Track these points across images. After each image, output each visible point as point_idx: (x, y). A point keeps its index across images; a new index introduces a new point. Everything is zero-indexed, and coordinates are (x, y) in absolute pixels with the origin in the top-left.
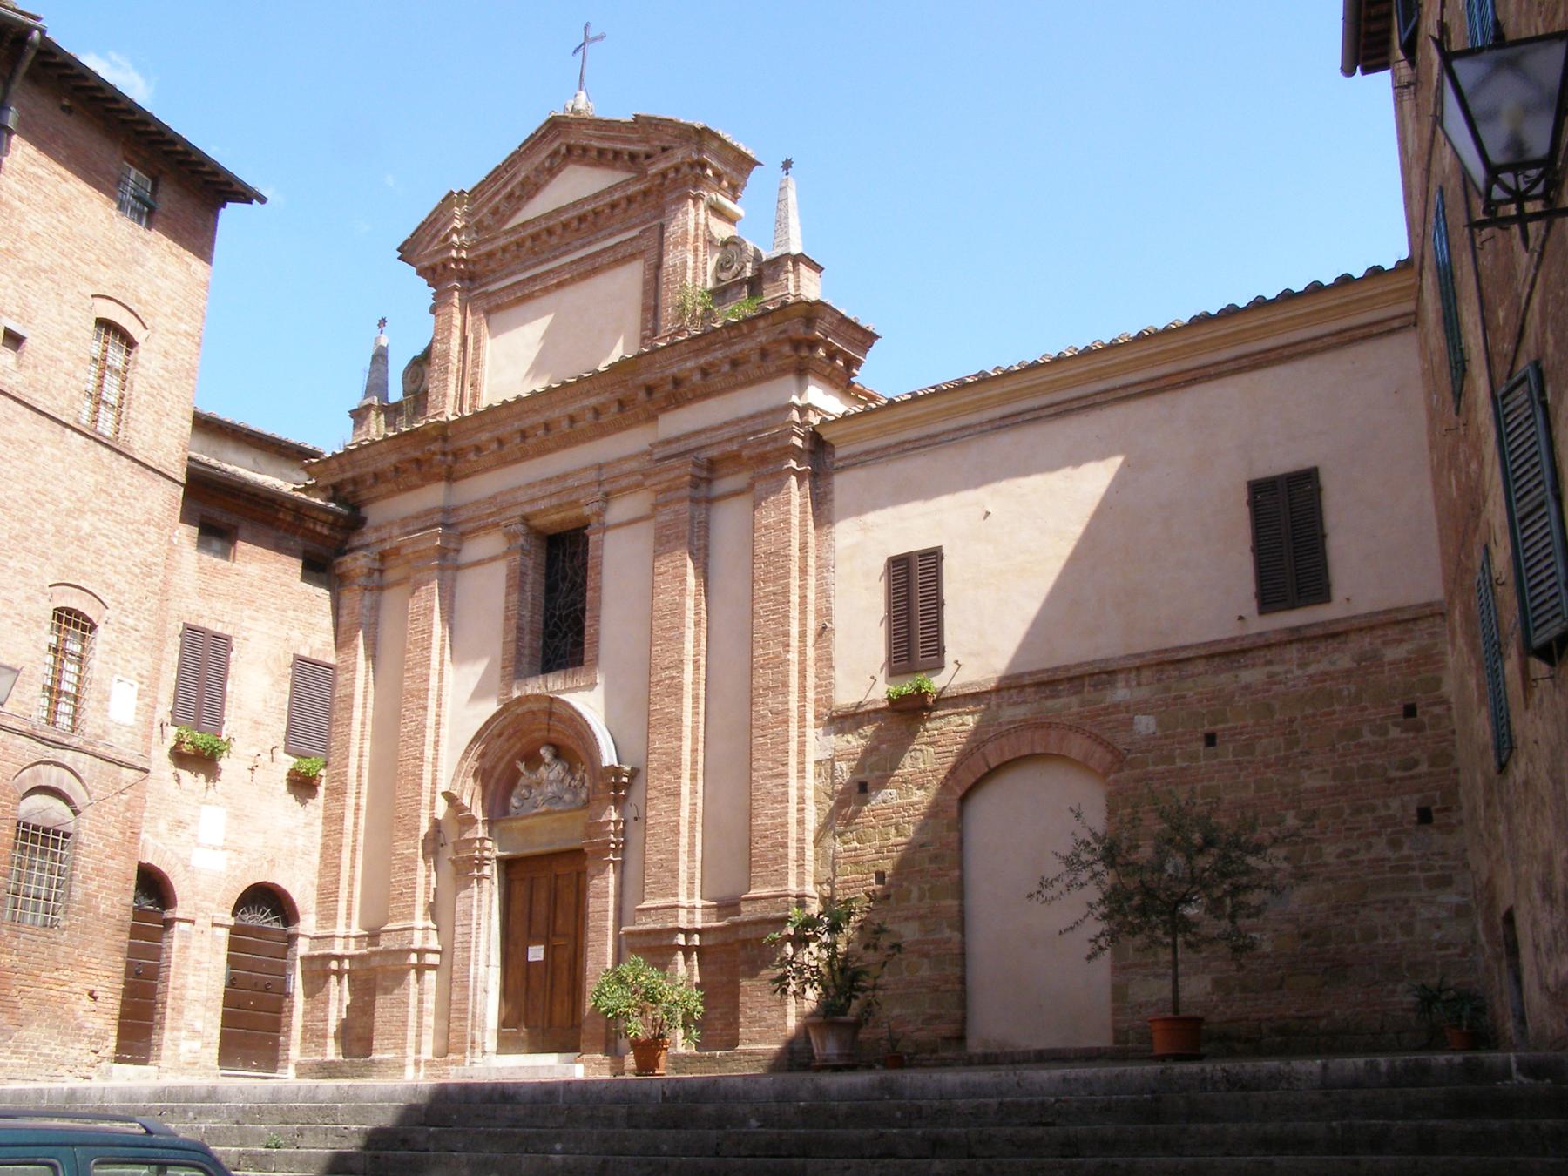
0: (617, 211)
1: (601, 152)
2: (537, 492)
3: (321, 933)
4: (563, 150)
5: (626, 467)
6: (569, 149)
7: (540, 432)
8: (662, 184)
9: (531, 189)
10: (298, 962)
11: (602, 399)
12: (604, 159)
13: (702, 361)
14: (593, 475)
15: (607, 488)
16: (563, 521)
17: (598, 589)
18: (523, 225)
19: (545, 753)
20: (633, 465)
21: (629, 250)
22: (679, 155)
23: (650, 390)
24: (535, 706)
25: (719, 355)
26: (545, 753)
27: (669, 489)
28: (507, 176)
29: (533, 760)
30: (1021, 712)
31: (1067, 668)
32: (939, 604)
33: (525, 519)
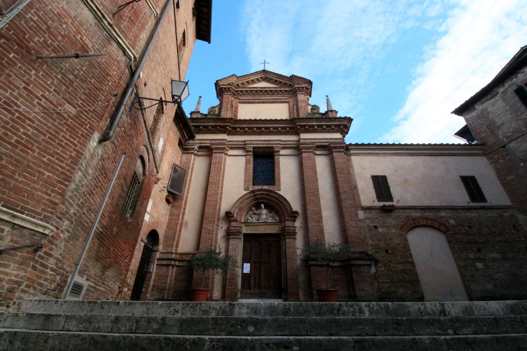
1: (276, 81)
2: (260, 142)
3: (165, 251)
9: (253, 82)
12: (275, 82)
17: (279, 168)
19: (263, 205)
21: (285, 100)
25: (324, 123)
26: (263, 205)
27: (306, 149)
31: (428, 206)
33: (254, 148)
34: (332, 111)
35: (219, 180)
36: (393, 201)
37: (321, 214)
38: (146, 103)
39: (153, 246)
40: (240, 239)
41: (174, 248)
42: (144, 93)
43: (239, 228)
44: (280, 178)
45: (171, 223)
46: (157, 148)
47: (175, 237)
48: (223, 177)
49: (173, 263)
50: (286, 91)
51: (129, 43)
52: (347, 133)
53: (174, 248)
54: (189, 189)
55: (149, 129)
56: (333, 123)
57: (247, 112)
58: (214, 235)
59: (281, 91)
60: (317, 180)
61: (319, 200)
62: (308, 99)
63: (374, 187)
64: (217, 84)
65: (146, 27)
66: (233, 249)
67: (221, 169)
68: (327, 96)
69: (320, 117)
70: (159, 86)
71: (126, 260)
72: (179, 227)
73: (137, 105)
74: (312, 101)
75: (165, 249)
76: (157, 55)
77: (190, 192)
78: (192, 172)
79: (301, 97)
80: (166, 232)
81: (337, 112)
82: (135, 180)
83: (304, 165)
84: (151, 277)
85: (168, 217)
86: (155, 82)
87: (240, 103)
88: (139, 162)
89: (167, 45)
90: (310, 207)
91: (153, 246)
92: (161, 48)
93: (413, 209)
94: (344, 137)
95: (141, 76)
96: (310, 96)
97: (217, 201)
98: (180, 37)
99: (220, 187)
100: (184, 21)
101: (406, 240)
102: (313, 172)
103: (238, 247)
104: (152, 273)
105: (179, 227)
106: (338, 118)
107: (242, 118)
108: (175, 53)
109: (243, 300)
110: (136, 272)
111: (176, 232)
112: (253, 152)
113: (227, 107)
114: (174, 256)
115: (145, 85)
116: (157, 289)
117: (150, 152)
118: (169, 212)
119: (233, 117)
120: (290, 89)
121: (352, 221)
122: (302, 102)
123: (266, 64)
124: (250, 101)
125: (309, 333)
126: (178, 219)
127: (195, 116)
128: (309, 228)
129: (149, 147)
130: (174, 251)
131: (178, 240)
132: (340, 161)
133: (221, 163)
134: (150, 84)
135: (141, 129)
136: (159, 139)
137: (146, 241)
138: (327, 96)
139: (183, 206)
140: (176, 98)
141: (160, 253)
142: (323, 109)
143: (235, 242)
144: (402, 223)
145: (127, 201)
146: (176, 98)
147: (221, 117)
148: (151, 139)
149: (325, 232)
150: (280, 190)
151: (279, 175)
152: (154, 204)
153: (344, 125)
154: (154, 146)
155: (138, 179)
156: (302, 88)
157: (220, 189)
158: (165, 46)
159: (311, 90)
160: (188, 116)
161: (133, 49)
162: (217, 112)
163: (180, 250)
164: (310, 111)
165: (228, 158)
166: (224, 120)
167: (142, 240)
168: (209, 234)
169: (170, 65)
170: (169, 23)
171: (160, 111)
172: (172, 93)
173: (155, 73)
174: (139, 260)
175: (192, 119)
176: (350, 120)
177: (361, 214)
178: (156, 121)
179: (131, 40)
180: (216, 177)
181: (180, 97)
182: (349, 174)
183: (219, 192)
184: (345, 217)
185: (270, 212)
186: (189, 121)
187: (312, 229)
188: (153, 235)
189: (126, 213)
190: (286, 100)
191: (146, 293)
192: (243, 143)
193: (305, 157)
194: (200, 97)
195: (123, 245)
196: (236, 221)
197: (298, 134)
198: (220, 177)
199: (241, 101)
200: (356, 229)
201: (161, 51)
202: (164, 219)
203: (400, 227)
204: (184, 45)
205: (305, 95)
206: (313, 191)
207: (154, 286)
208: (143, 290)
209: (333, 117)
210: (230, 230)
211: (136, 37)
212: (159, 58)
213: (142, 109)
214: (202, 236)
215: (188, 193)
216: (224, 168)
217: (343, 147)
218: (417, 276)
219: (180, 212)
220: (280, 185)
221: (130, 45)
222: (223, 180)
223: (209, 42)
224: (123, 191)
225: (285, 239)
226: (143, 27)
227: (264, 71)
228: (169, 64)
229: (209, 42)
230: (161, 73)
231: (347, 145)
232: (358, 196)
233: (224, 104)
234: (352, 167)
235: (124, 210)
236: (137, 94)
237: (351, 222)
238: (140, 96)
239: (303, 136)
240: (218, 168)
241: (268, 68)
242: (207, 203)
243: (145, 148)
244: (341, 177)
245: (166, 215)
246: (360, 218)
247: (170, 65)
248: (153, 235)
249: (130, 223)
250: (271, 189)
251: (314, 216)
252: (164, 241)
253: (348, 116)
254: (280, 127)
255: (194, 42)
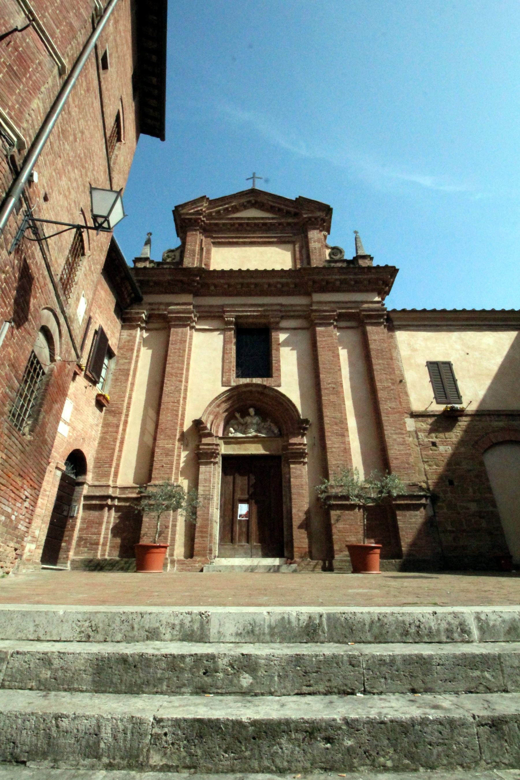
0: (280, 226)
1: (272, 207)
3: (97, 483)
4: (253, 202)
5: (294, 308)
6: (256, 202)
7: (253, 286)
8: (307, 222)
9: (236, 209)
10: (82, 499)
11: (289, 280)
12: (271, 209)
13: (343, 277)
14: (278, 308)
15: (284, 314)
16: (252, 323)
18: (237, 218)
19: (252, 411)
20: (299, 308)
22: (319, 214)
23: (314, 282)
24: (254, 389)
25: (351, 277)
26: (252, 411)
28: (227, 201)
29: (244, 413)
30: (501, 424)
32: (455, 381)
33: (237, 317)
34: (364, 257)
35: (182, 369)
36: (461, 403)
37: (347, 424)
38: (48, 230)
39: (77, 475)
40: (216, 463)
41: (111, 478)
42: (44, 211)
43: (215, 447)
44: (279, 366)
45: (106, 439)
46: (75, 314)
47: (112, 460)
48: (188, 364)
49: (109, 502)
50: (289, 224)
51: (9, 114)
52: (388, 293)
53: (111, 478)
54: (133, 384)
55: (57, 279)
56: (366, 277)
57: (225, 258)
58: (175, 458)
59: (280, 224)
60: (340, 370)
61: (344, 401)
62: (325, 237)
63: (431, 381)
64: (177, 212)
65: (43, 89)
66: (205, 480)
67: (185, 351)
68: (356, 232)
69: (345, 265)
70: (73, 205)
71: (26, 504)
72: (118, 444)
73: (29, 233)
74: (332, 240)
75: (97, 480)
76: (67, 147)
77: (135, 388)
78: (138, 356)
79: (314, 235)
80: (98, 452)
81: (372, 259)
82: (35, 369)
83: (318, 344)
84: (75, 525)
85: (100, 428)
86: (65, 196)
87: (214, 243)
88: (41, 338)
89: (87, 133)
90: (327, 412)
91: (77, 475)
92: (75, 135)
93: (493, 415)
94: (383, 299)
95: (36, 178)
96: (329, 234)
97: (179, 404)
98: (110, 122)
99: (184, 380)
100: (118, 94)
101: (482, 464)
102: (333, 357)
103: (213, 476)
104: (76, 518)
105: (118, 444)
106: (374, 267)
107: (219, 268)
108: (101, 150)
109: (223, 559)
110: (49, 519)
111: (113, 453)
112: (236, 324)
113: (194, 251)
114: (110, 492)
115: (46, 199)
116: (85, 543)
117: (62, 320)
118: (102, 421)
119: (203, 266)
120: (296, 220)
121: (396, 434)
122: (315, 242)
123: (257, 181)
124: (231, 240)
125: (368, 689)
126: (117, 432)
127: (140, 265)
128: (328, 446)
129: (58, 311)
130: (111, 483)
131: (118, 465)
132: (376, 337)
133: (185, 341)
134: (54, 197)
135: (41, 279)
136: (78, 300)
137: (64, 468)
138: (356, 232)
139: (124, 411)
140: (100, 220)
141: (89, 486)
142: (349, 255)
143: (208, 469)
144: (476, 438)
145: (23, 406)
146: (100, 220)
147: (184, 266)
148: (62, 298)
149: (352, 450)
150: (279, 386)
151: (279, 361)
152: (77, 409)
153: (383, 278)
154: (69, 311)
155: (41, 368)
156: (316, 219)
157: (183, 383)
158: (82, 133)
159: (330, 222)
160: (130, 264)
161: (19, 126)
162: (177, 259)
163: (121, 482)
164: (328, 258)
165: (195, 334)
166: (189, 271)
167: (57, 468)
168: (167, 455)
169: (94, 170)
170: (88, 90)
171: (78, 250)
172: (92, 210)
173: (64, 178)
174: (53, 499)
175: (136, 269)
176: (392, 271)
177: (410, 424)
178: (71, 267)
179: (12, 108)
180: (176, 365)
181: (106, 218)
182: (392, 359)
183: (183, 388)
184: (385, 428)
185: (264, 420)
186: (132, 273)
187: (331, 448)
188: (76, 460)
189: (21, 426)
190: (290, 239)
191: (68, 550)
192: (221, 310)
193: (322, 332)
194: (151, 234)
195: (18, 480)
196: (210, 435)
197: (309, 294)
198: (183, 364)
199: (217, 240)
200: (402, 447)
201: (75, 140)
202: (93, 433)
203: (472, 443)
204: (119, 140)
205: (321, 231)
206: (334, 386)
207: (80, 539)
208: (63, 544)
209: (366, 266)
210: (200, 449)
211: (24, 104)
212: (71, 154)
213: (40, 239)
214: (155, 459)
215: (132, 390)
216: (190, 350)
217: (381, 316)
218: (498, 520)
219: (119, 420)
220: (279, 376)
221: (11, 118)
222: (188, 370)
223: (163, 138)
224: (11, 388)
225: (289, 464)
226: (36, 88)
227: (253, 192)
228: (91, 168)
229: (163, 138)
230: (76, 180)
231: (388, 312)
232: (406, 394)
233: (188, 247)
234: (396, 347)
235: (18, 420)
236: (29, 215)
237: (395, 436)
238: (36, 217)
239: (317, 297)
240: (180, 349)
241: (260, 186)
242: (162, 406)
243: (50, 313)
244: (379, 364)
245: (97, 425)
246: (408, 429)
247: (94, 170)
248: (76, 460)
249: (30, 442)
250: (265, 383)
251: (335, 427)
252: (95, 467)
253: (390, 264)
254: (280, 283)
255: (137, 137)
